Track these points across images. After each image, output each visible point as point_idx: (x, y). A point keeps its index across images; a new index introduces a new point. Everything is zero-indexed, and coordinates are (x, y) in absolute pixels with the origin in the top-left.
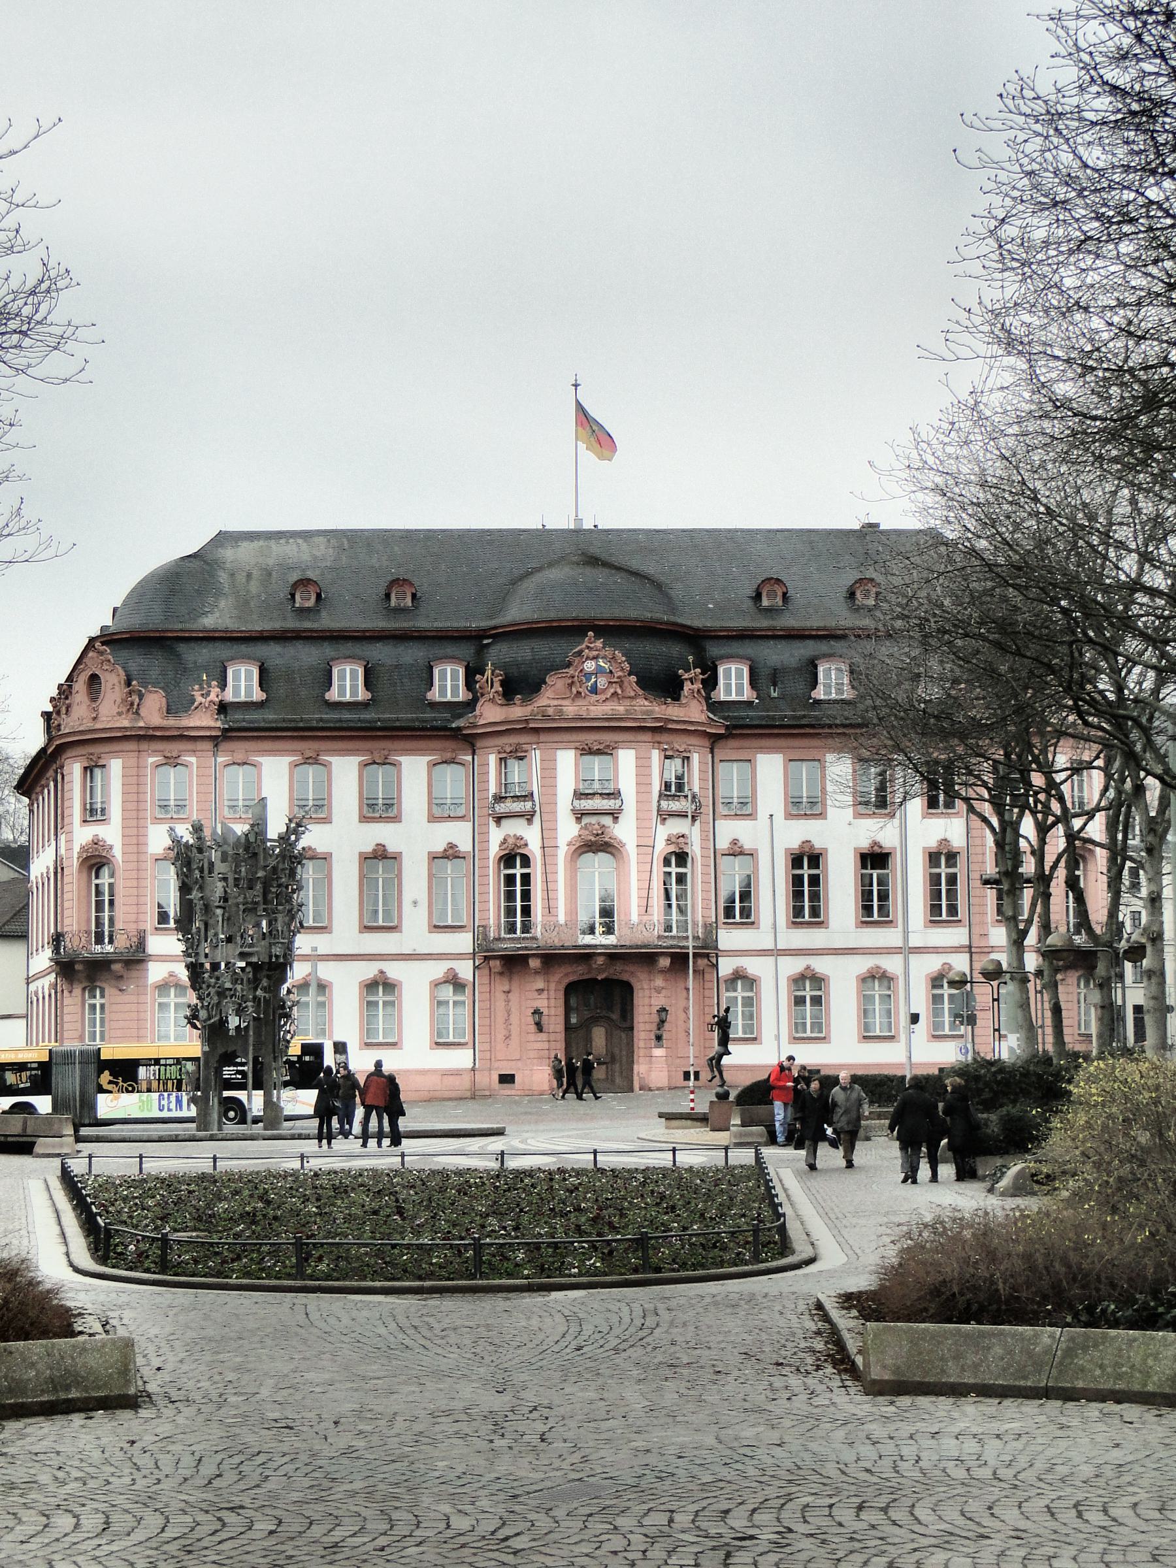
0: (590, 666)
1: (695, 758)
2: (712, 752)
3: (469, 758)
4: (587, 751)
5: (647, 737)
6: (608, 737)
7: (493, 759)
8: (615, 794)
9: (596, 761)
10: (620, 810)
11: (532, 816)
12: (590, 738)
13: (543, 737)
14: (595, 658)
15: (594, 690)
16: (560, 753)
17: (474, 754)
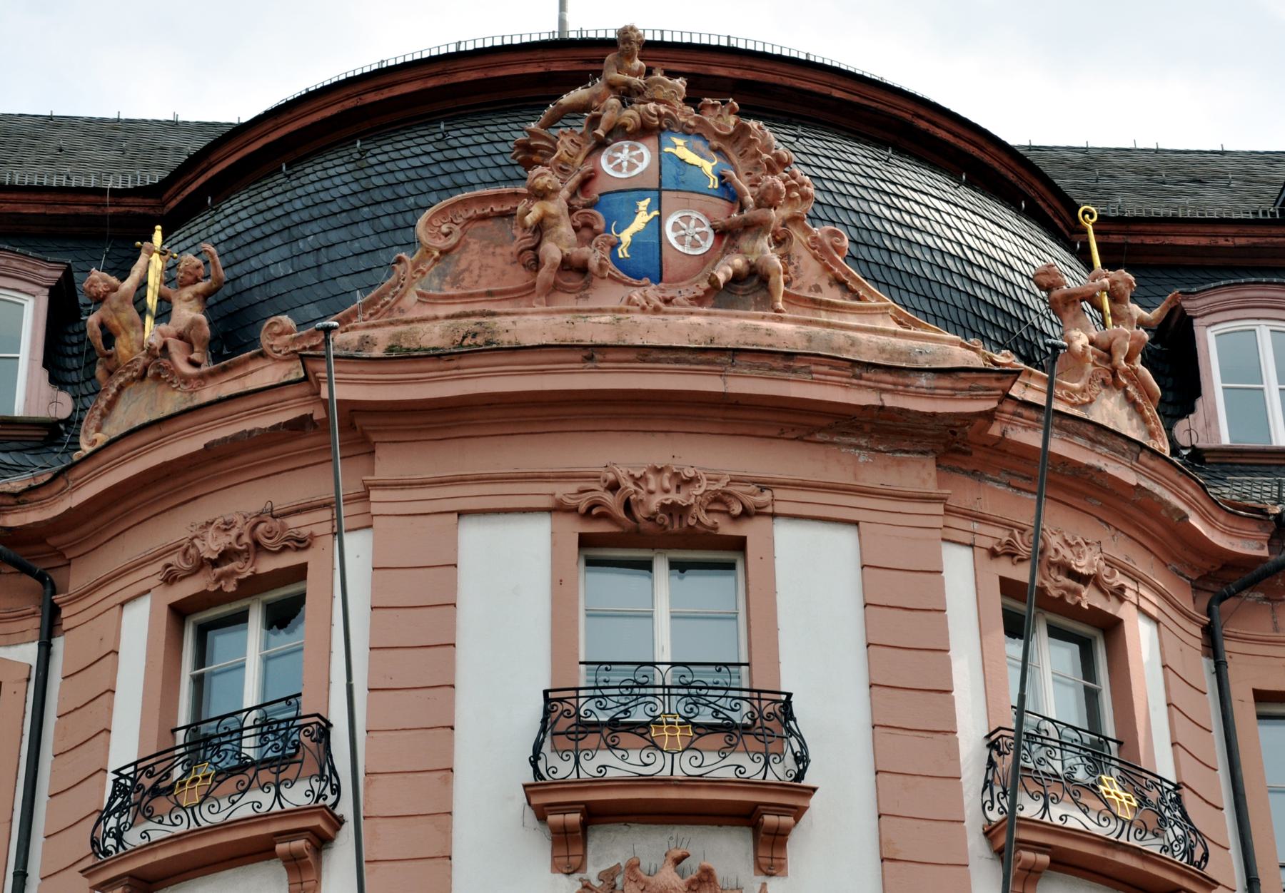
0: (627, 162)
1: (1143, 640)
2: (1212, 643)
3: (28, 653)
4: (617, 537)
5: (919, 474)
6: (715, 461)
7: (138, 626)
8: (775, 719)
9: (663, 590)
10: (797, 793)
11: (321, 842)
12: (644, 463)
13: (391, 463)
14: (644, 131)
15: (649, 264)
16: (475, 539)
17: (51, 627)
